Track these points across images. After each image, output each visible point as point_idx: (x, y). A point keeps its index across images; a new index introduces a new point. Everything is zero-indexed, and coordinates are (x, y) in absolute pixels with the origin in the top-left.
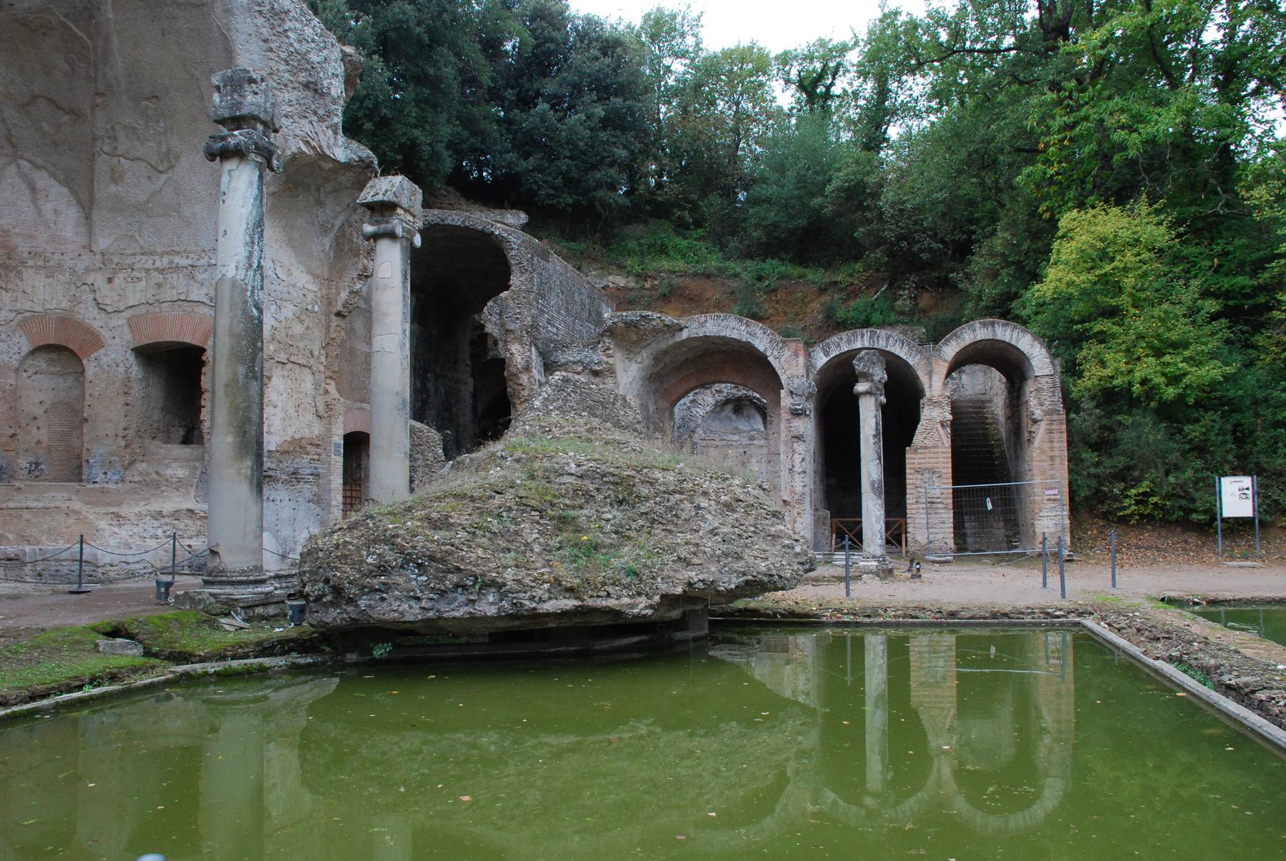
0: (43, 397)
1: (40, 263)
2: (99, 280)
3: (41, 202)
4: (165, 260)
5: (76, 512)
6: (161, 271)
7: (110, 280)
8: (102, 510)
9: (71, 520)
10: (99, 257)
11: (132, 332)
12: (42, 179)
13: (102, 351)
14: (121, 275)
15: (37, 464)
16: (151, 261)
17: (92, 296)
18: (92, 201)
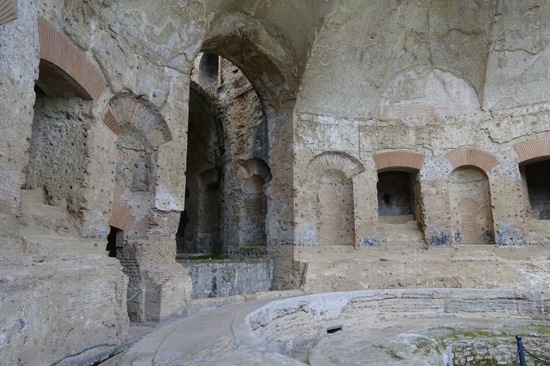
0: (457, 196)
1: (453, 121)
2: (491, 126)
3: (449, 89)
4: (536, 108)
5: (503, 263)
6: (535, 114)
7: (498, 125)
8: (520, 262)
9: (500, 268)
10: (488, 113)
11: (518, 153)
12: (448, 77)
13: (499, 166)
14: (505, 121)
15: (458, 234)
16: (525, 111)
17: (487, 135)
18: (483, 81)
